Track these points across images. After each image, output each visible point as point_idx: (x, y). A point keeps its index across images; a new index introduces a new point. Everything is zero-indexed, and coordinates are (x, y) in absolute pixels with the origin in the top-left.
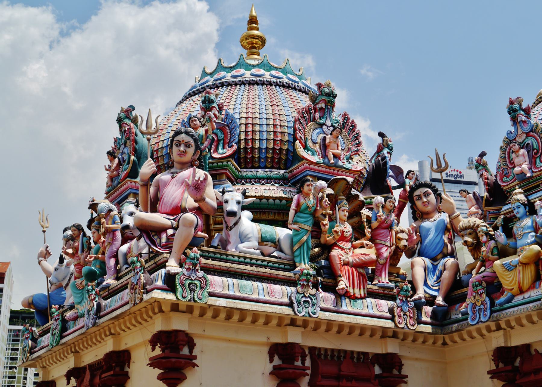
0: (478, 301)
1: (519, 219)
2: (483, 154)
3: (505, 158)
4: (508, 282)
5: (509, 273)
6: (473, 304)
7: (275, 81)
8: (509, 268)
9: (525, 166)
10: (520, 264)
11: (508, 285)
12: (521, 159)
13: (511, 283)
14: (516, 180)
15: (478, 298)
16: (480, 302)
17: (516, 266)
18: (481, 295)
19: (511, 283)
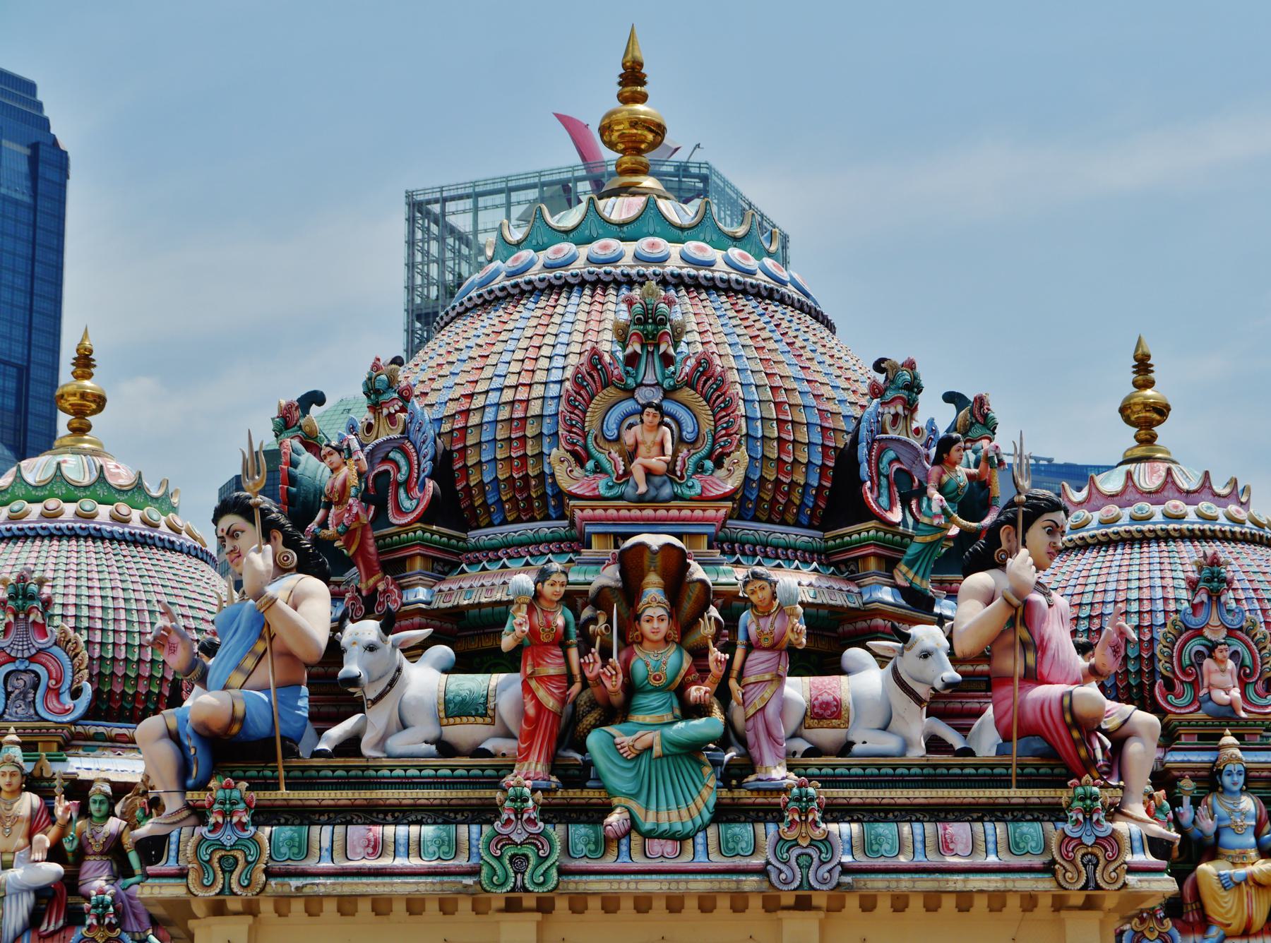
0: (1151, 930)
1: (1225, 790)
2: (316, 398)
3: (1172, 657)
4: (1223, 911)
5: (1225, 893)
6: (1136, 932)
7: (693, 272)
8: (1229, 884)
9: (1236, 693)
10: (1251, 883)
11: (1221, 915)
12: (1228, 677)
13: (1227, 913)
14: (1199, 708)
15: (1153, 924)
16: (1156, 933)
17: (1238, 884)
18: (1160, 921)
19: (1227, 913)
